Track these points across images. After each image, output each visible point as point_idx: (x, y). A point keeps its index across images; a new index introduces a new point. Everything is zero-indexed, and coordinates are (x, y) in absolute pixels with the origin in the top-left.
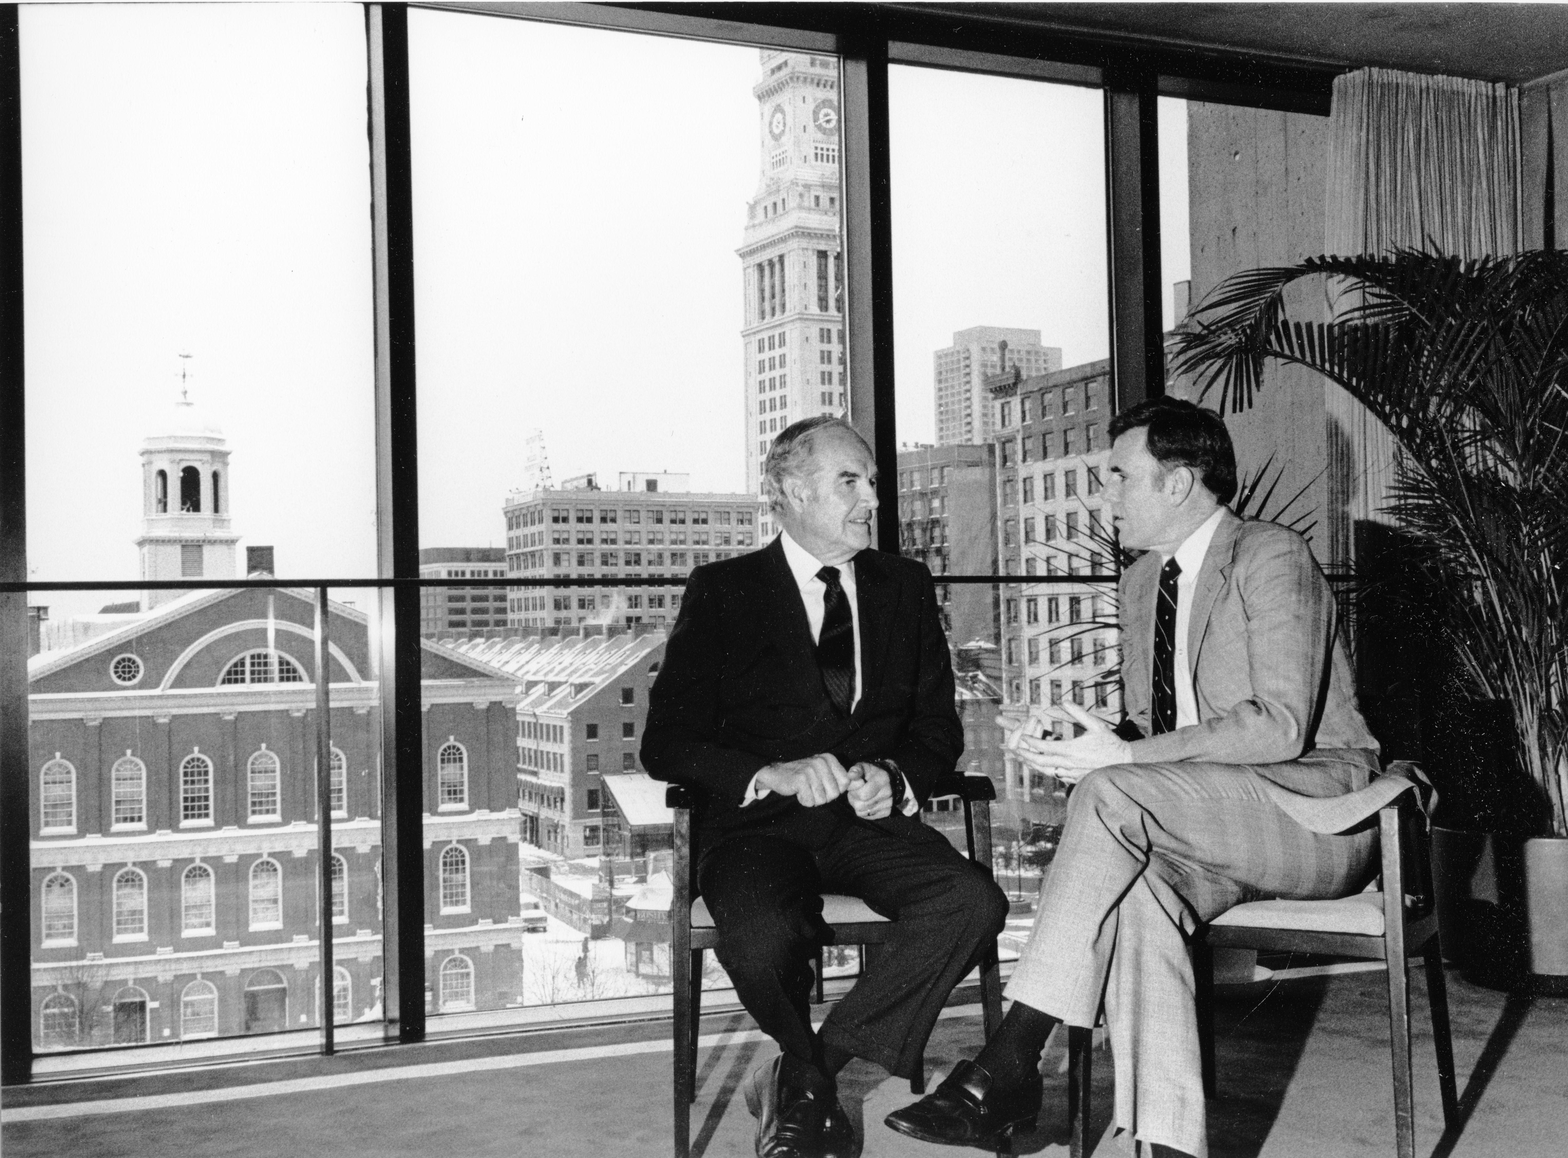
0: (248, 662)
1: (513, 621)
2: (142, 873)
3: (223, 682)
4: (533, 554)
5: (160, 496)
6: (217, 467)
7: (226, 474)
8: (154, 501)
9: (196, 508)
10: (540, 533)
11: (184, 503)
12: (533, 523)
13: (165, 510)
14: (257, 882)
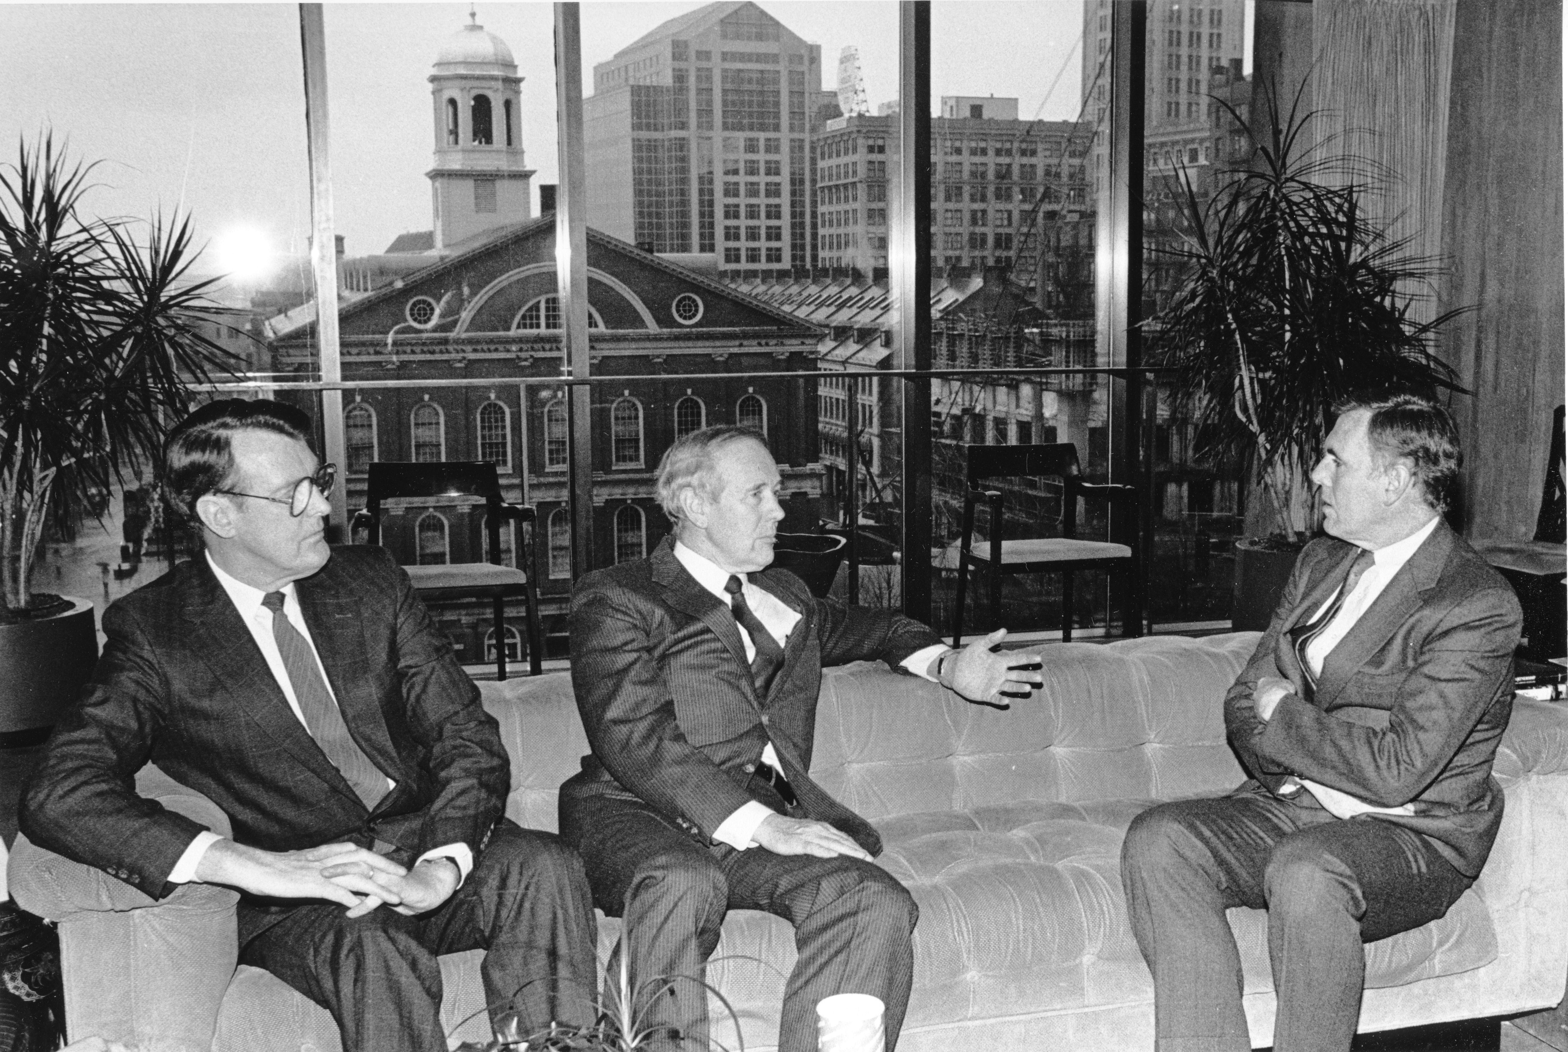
0: (543, 306)
1: (824, 259)
2: (443, 518)
3: (518, 327)
4: (845, 186)
5: (451, 127)
6: (509, 95)
7: (519, 102)
8: (445, 134)
9: (489, 141)
10: (854, 164)
11: (476, 135)
12: (846, 153)
13: (456, 142)
14: (557, 529)
